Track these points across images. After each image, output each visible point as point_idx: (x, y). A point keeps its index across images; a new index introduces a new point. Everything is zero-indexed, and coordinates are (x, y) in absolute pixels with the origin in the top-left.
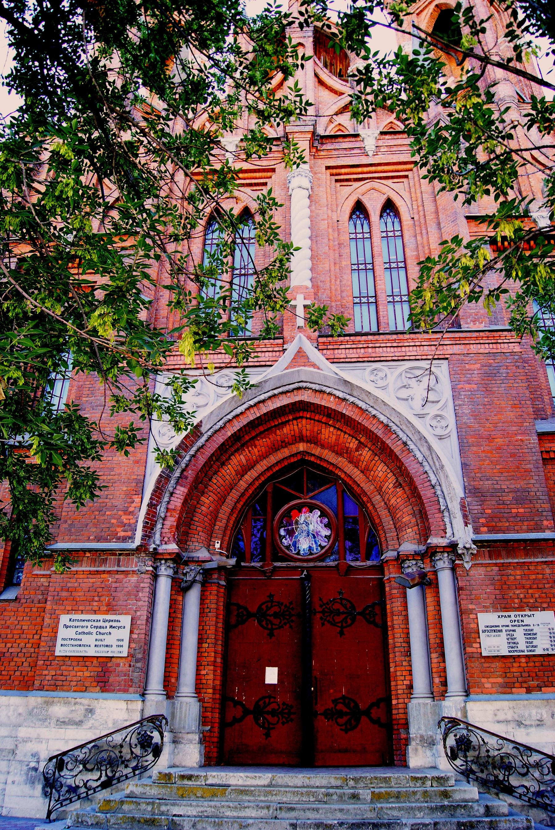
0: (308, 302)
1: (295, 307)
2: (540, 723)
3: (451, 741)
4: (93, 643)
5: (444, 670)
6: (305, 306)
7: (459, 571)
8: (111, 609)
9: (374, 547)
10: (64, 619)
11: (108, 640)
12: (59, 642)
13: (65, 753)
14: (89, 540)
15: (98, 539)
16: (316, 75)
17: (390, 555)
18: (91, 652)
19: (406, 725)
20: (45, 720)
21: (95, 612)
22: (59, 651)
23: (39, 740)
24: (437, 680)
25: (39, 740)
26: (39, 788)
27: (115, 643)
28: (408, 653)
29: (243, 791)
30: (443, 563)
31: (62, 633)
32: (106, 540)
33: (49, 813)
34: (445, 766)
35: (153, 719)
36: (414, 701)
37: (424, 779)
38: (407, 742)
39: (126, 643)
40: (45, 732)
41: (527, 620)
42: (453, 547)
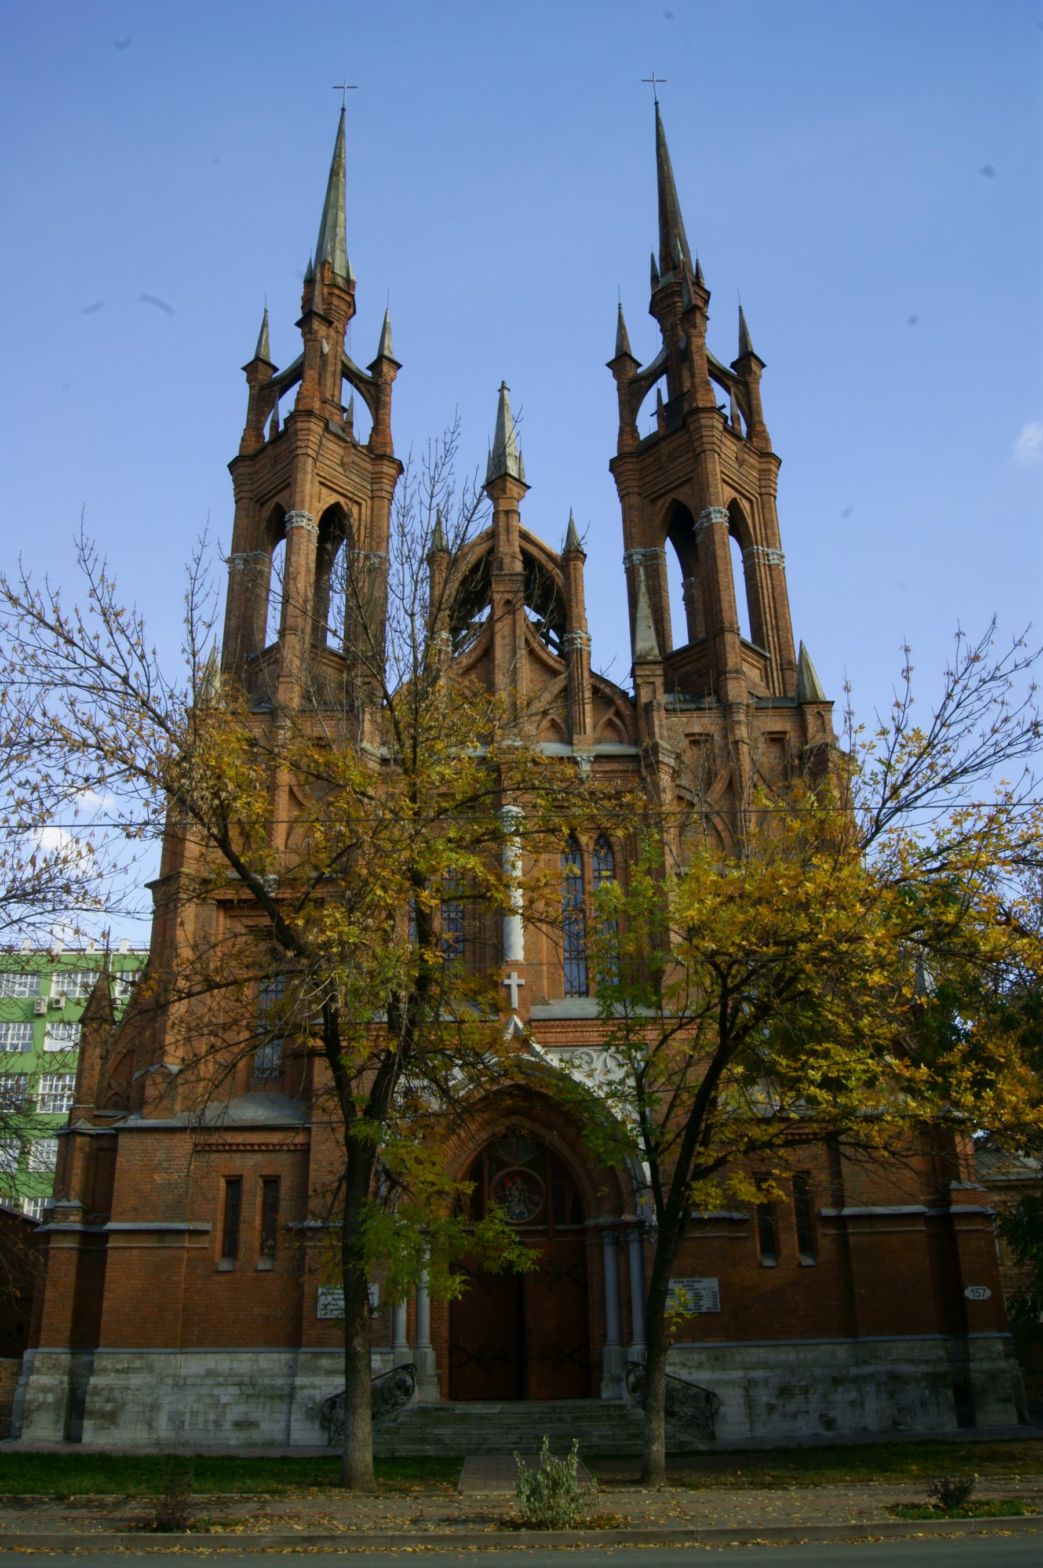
0: (523, 982)
1: (509, 986)
2: (700, 1366)
3: (632, 1379)
5: (631, 1323)
6: (519, 986)
7: (646, 1245)
9: (579, 1216)
13: (337, 1396)
16: (527, 641)
17: (590, 1222)
19: (600, 1366)
20: (316, 1371)
23: (313, 1387)
24: (625, 1331)
25: (313, 1387)
26: (317, 1426)
28: (603, 1307)
29: (482, 1417)
30: (633, 1236)
33: (330, 1440)
34: (627, 1398)
35: (405, 1367)
36: (607, 1348)
37: (609, 1407)
38: (601, 1379)
40: (317, 1380)
41: (696, 1285)
42: (640, 1224)
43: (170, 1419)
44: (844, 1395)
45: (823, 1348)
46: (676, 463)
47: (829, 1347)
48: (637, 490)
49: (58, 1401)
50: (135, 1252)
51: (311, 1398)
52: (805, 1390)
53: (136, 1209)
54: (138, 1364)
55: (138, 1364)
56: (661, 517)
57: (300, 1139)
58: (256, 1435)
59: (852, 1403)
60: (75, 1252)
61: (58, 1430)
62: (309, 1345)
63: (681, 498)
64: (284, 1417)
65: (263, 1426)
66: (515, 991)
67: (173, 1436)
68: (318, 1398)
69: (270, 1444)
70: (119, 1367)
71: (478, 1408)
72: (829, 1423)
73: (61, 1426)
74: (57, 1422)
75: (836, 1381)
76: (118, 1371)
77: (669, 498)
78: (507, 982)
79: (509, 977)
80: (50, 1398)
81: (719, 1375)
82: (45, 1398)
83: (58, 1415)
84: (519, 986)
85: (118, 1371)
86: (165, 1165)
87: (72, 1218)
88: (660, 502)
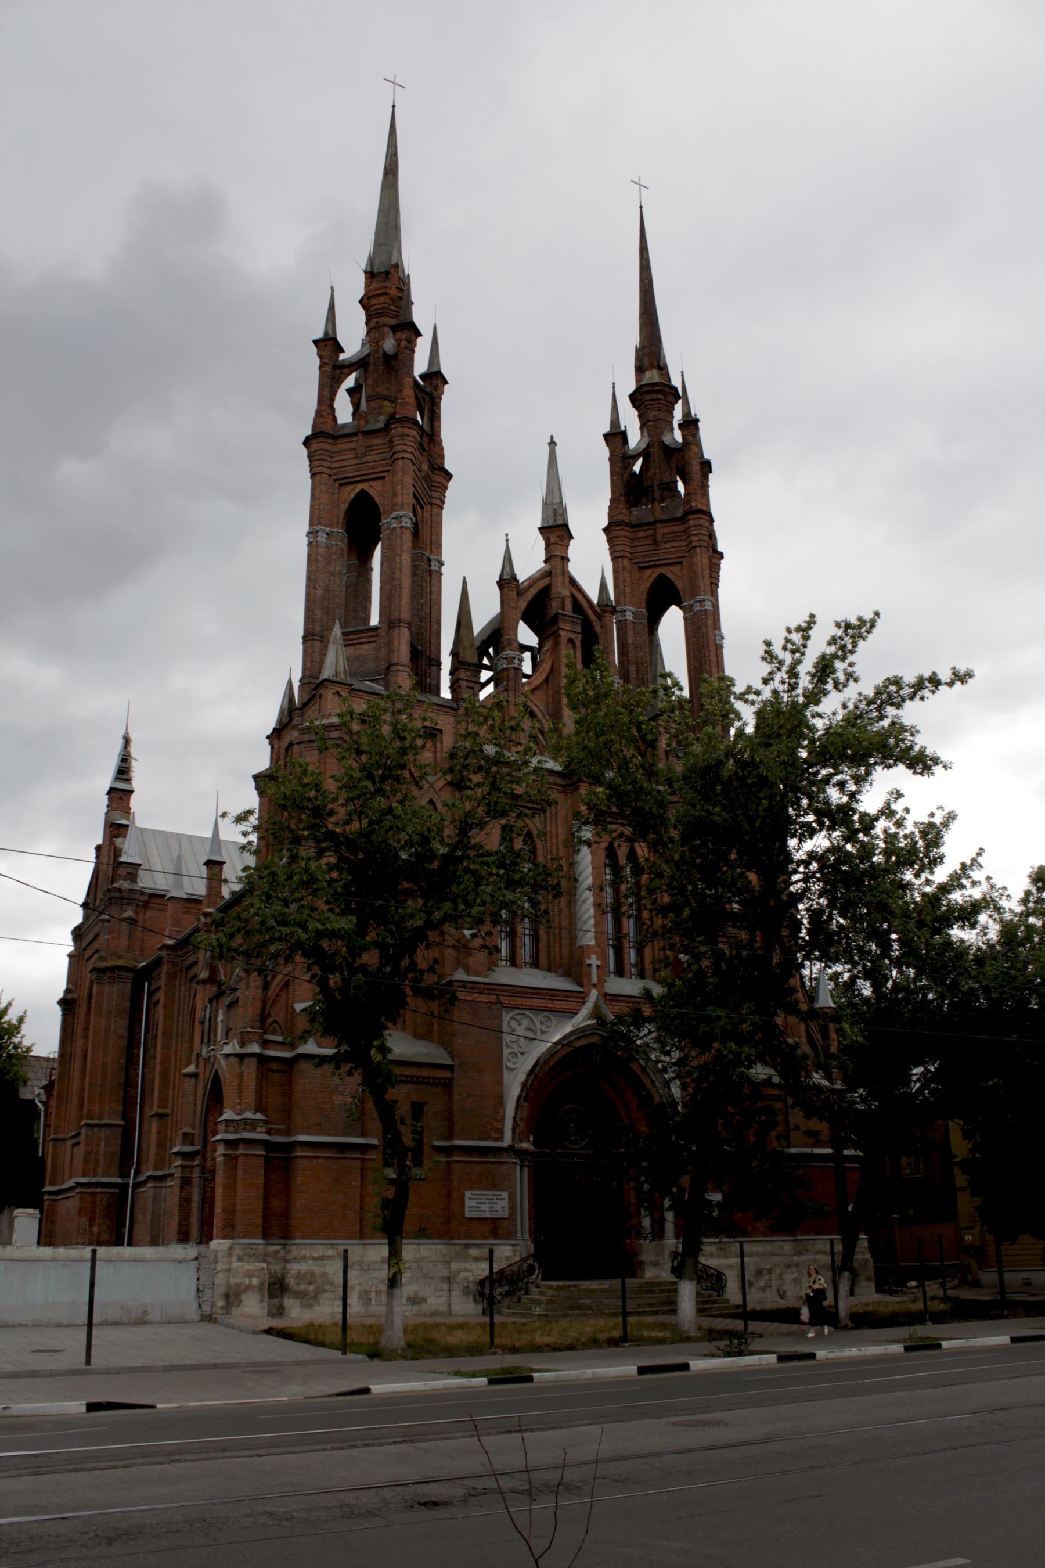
0: (599, 963)
1: (590, 965)
4: (488, 1209)
6: (598, 966)
8: (493, 1186)
10: (468, 1194)
11: (498, 1207)
12: (467, 1209)
14: (474, 1139)
15: (481, 1139)
18: (487, 1215)
20: (466, 1258)
21: (485, 1189)
22: (467, 1214)
27: (500, 1209)
31: (468, 1203)
32: (485, 1140)
39: (507, 1209)
40: (468, 1265)
43: (360, 1297)
44: (789, 1277)
45: (776, 1243)
46: (668, 545)
47: (780, 1243)
48: (629, 555)
49: (262, 1284)
50: (321, 1161)
51: (466, 1278)
52: (770, 1272)
53: (319, 1125)
54: (330, 1252)
55: (330, 1252)
56: (648, 584)
57: (447, 1074)
58: (424, 1307)
59: (795, 1280)
60: (263, 1159)
61: (263, 1308)
62: (459, 1238)
63: (669, 575)
64: (445, 1293)
65: (430, 1301)
66: (594, 968)
67: (363, 1310)
68: (471, 1279)
69: (434, 1314)
70: (316, 1255)
71: (594, 1285)
72: (782, 1295)
73: (265, 1304)
74: (262, 1301)
75: (788, 1266)
76: (315, 1259)
77: (661, 570)
78: (589, 962)
79: (589, 958)
80: (255, 1281)
81: (724, 1261)
82: (250, 1282)
83: (263, 1295)
84: (598, 966)
85: (315, 1259)
86: (341, 1089)
87: (259, 1129)
88: (649, 572)
